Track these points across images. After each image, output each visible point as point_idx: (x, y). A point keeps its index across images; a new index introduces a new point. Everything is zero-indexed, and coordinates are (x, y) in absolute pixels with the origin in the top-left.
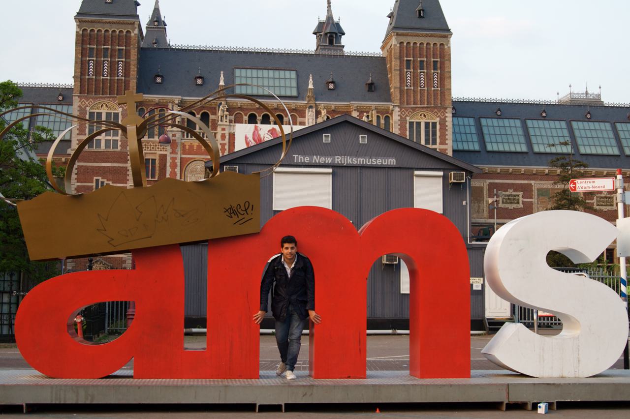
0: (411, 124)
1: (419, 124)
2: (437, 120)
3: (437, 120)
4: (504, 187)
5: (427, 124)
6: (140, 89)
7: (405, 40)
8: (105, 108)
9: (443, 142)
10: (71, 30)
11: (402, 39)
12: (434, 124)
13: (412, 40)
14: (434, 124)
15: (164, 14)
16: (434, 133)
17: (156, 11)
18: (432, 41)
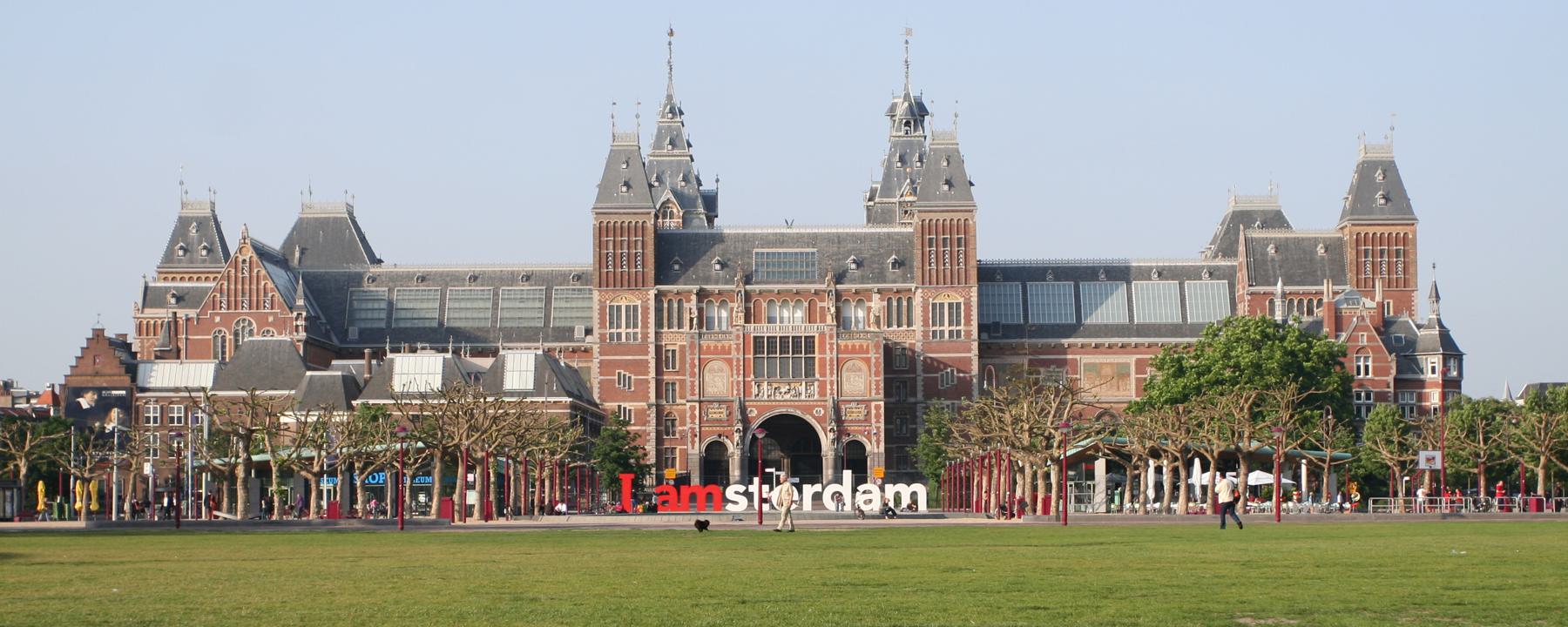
0: (934, 305)
1: (942, 305)
2: (961, 300)
3: (961, 300)
4: (1046, 363)
5: (950, 305)
6: (658, 282)
7: (927, 217)
8: (625, 300)
9: (968, 322)
10: (588, 223)
11: (924, 216)
12: (958, 305)
13: (934, 216)
14: (958, 305)
15: (676, 101)
16: (958, 315)
17: (670, 97)
18: (956, 216)
